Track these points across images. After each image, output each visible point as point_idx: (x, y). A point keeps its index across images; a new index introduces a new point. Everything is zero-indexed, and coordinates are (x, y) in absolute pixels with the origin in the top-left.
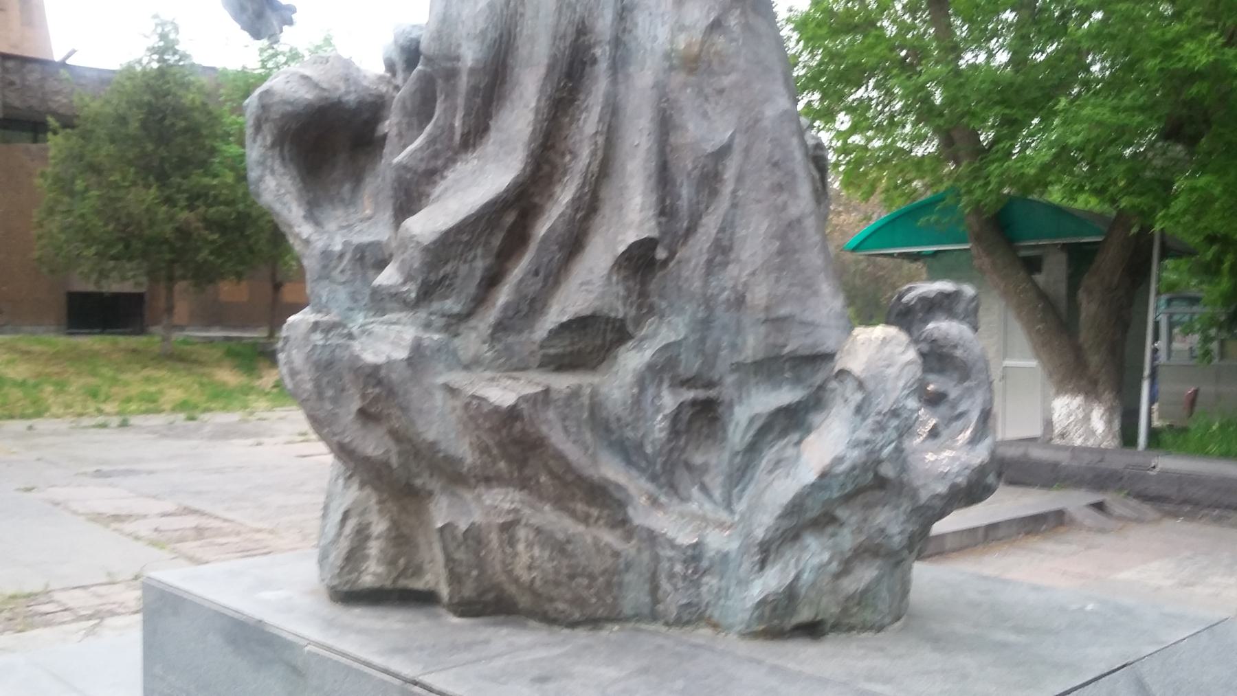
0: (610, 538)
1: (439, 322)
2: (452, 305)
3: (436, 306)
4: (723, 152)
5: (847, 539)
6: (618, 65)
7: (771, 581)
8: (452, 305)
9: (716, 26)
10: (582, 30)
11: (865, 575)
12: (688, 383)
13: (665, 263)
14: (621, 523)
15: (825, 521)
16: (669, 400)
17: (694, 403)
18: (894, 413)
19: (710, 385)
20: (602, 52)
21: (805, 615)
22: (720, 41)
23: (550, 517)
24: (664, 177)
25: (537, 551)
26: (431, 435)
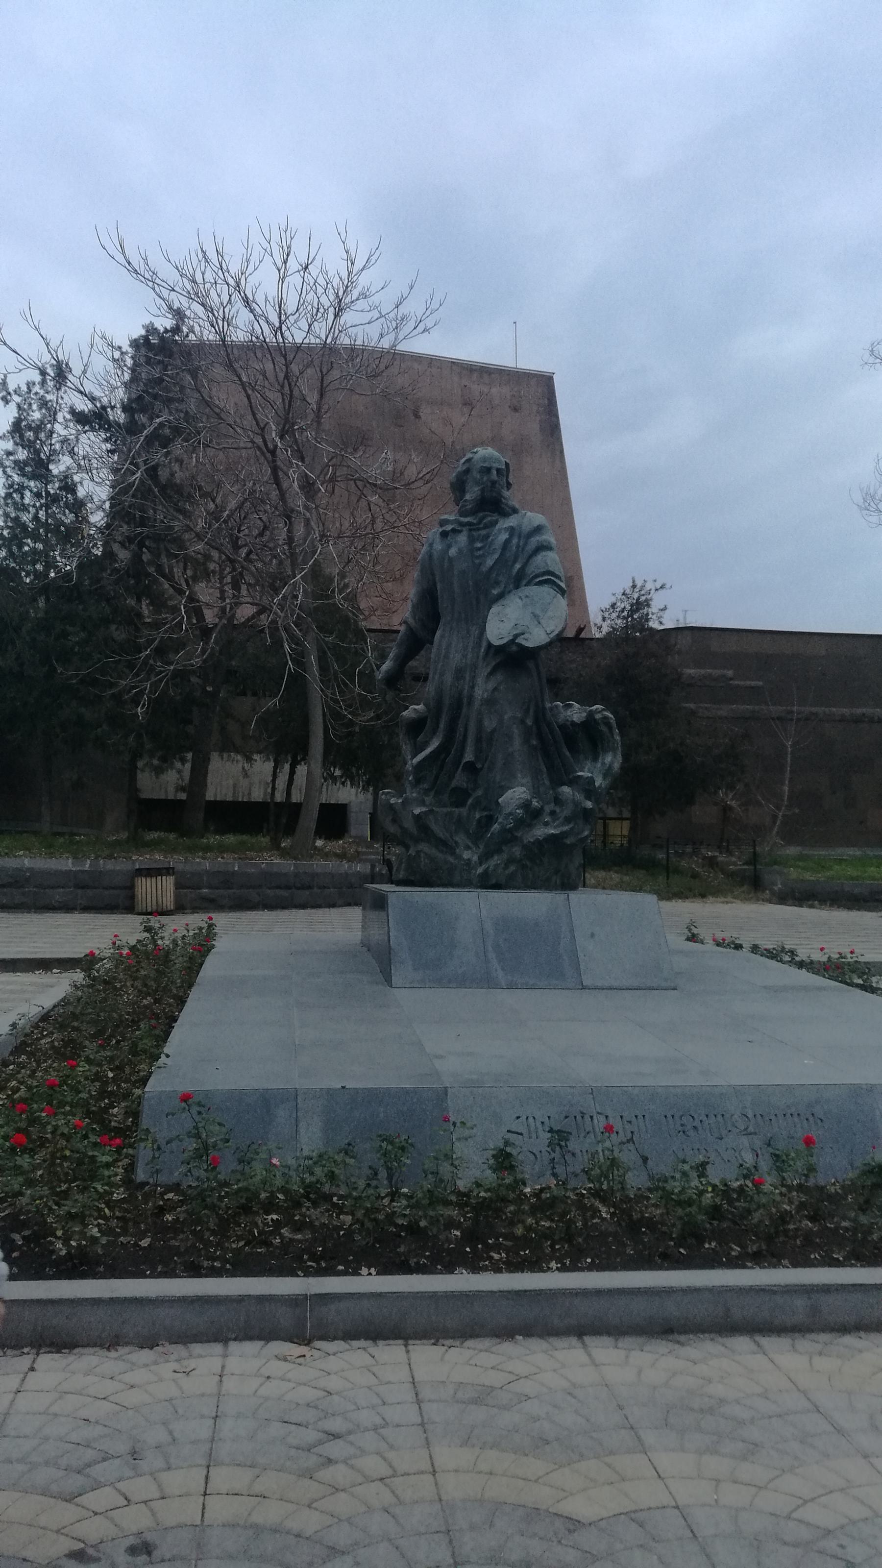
0: (451, 859)
1: (422, 792)
2: (426, 786)
3: (421, 786)
4: (494, 731)
5: (505, 856)
6: (470, 703)
7: (480, 870)
8: (426, 786)
9: (495, 689)
10: (460, 693)
11: (512, 868)
12: (484, 809)
13: (481, 769)
14: (453, 853)
15: (499, 851)
16: (477, 816)
17: (486, 816)
18: (510, 814)
19: (490, 810)
20: (465, 700)
21: (494, 881)
22: (496, 693)
23: (434, 852)
24: (478, 740)
25: (426, 860)
26: (406, 826)
